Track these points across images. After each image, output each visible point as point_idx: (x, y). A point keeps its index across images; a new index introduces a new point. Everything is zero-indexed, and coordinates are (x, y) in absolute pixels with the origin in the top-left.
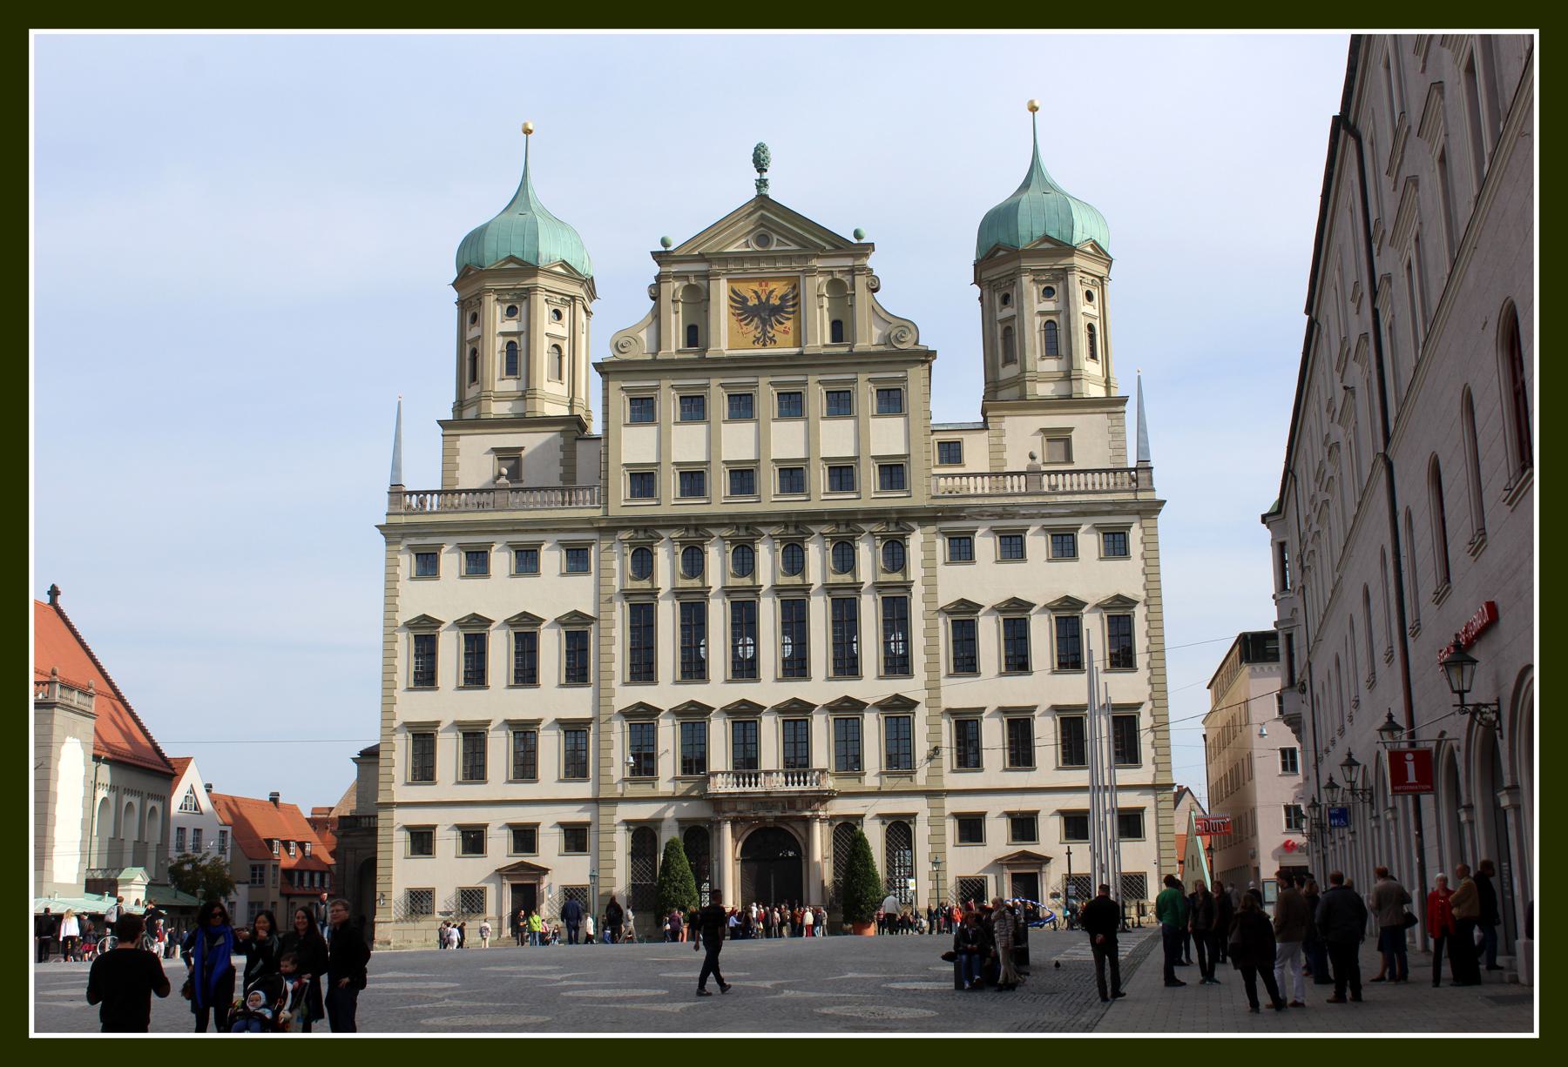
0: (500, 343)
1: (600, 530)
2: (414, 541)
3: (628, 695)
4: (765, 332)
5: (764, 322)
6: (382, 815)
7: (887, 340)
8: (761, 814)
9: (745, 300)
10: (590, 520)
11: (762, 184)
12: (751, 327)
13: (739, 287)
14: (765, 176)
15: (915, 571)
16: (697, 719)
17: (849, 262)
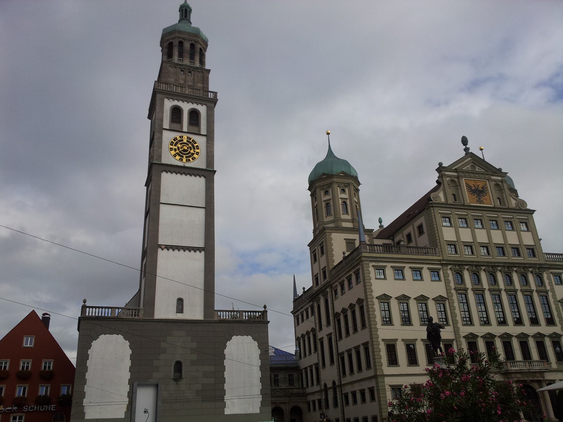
0: (340, 201)
1: (442, 264)
2: (374, 264)
3: (465, 330)
4: (480, 199)
5: (479, 195)
6: (380, 380)
7: (517, 204)
8: (525, 379)
9: (471, 187)
10: (440, 260)
11: (466, 150)
12: (475, 196)
13: (469, 182)
14: (468, 146)
15: (548, 288)
16: (490, 340)
17: (500, 178)
